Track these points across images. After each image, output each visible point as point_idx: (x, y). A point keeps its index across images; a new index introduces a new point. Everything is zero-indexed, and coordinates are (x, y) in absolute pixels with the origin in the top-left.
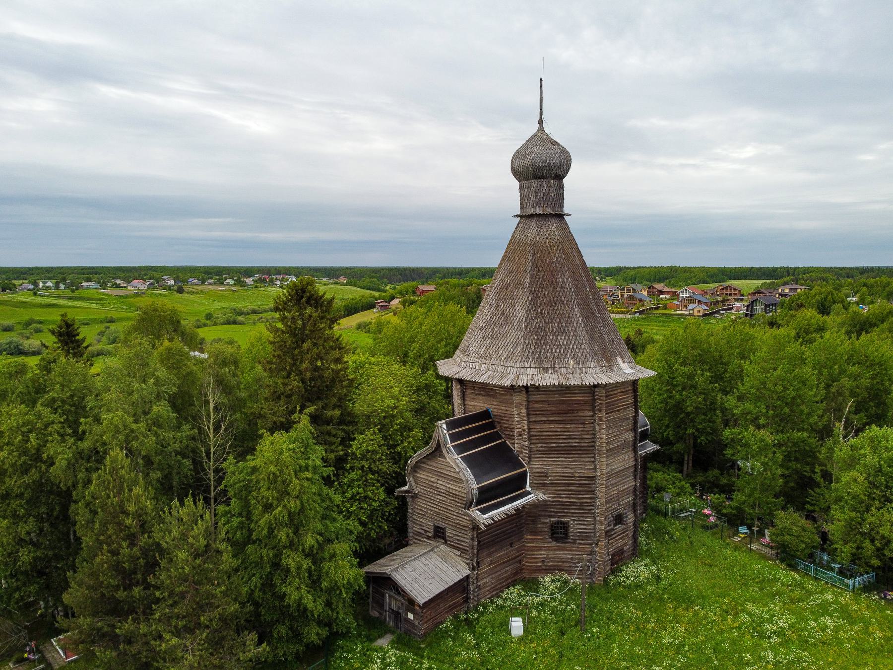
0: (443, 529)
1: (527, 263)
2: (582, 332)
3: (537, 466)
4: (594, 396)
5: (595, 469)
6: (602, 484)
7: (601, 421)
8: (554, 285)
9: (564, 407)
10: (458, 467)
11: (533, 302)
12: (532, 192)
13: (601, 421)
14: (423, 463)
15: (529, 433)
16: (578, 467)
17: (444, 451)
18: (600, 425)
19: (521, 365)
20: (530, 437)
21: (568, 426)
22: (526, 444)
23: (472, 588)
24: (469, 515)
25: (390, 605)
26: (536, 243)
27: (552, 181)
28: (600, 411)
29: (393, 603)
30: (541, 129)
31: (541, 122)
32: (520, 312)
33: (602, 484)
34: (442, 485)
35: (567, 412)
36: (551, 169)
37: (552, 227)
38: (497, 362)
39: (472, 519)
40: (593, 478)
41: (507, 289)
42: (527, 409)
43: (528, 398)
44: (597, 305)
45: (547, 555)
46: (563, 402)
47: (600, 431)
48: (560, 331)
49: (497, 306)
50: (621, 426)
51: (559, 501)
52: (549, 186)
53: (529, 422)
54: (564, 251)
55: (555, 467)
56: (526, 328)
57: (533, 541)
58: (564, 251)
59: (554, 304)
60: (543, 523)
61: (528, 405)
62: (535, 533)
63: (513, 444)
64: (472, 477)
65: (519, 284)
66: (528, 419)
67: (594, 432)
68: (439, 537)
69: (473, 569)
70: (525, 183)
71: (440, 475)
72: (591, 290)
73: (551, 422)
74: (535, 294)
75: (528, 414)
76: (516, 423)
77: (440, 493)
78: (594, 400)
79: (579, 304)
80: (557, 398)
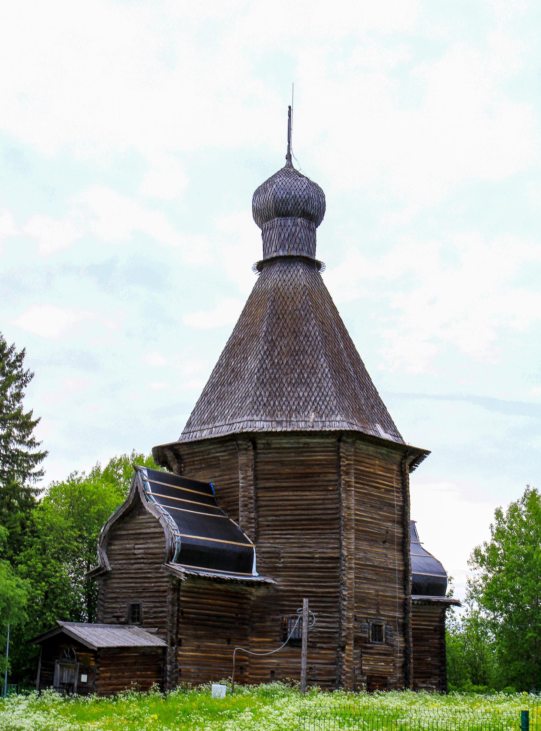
0: (138, 605)
1: (265, 311)
2: (328, 384)
3: (267, 545)
4: (338, 453)
5: (340, 548)
6: (350, 568)
7: (350, 486)
8: (296, 334)
9: (300, 469)
10: (159, 513)
11: (269, 353)
12: (274, 234)
13: (350, 486)
14: (120, 529)
15: (256, 501)
16: (317, 547)
17: (143, 500)
18: (347, 491)
19: (249, 418)
20: (257, 508)
21: (307, 493)
22: (252, 515)
23: (169, 667)
24: (167, 569)
25: (61, 678)
26: (276, 290)
27: (299, 220)
28: (347, 473)
29: (65, 674)
30: (289, 165)
31: (289, 157)
32: (253, 364)
33: (350, 568)
34: (140, 548)
35: (306, 476)
36: (297, 203)
37: (299, 274)
38: (222, 423)
39: (173, 575)
40: (337, 559)
41: (240, 344)
42: (255, 470)
43: (255, 458)
44: (353, 365)
45: (278, 664)
46: (302, 463)
47: (347, 499)
48: (299, 382)
49: (228, 364)
50: (380, 509)
51: (293, 591)
52: (295, 225)
53: (257, 489)
54: (311, 298)
55: (292, 546)
56: (258, 379)
57: (260, 645)
58: (311, 298)
59: (294, 354)
60: (273, 620)
61: (256, 467)
62: (262, 634)
63: (237, 520)
64: (174, 524)
65: (255, 335)
66: (255, 485)
67: (339, 500)
68: (134, 620)
69: (172, 645)
70: (268, 224)
71: (138, 536)
72: (346, 348)
73: (286, 489)
74: (272, 344)
75: (256, 478)
76: (241, 490)
77: (137, 559)
78: (340, 458)
79: (326, 355)
80: (293, 457)
